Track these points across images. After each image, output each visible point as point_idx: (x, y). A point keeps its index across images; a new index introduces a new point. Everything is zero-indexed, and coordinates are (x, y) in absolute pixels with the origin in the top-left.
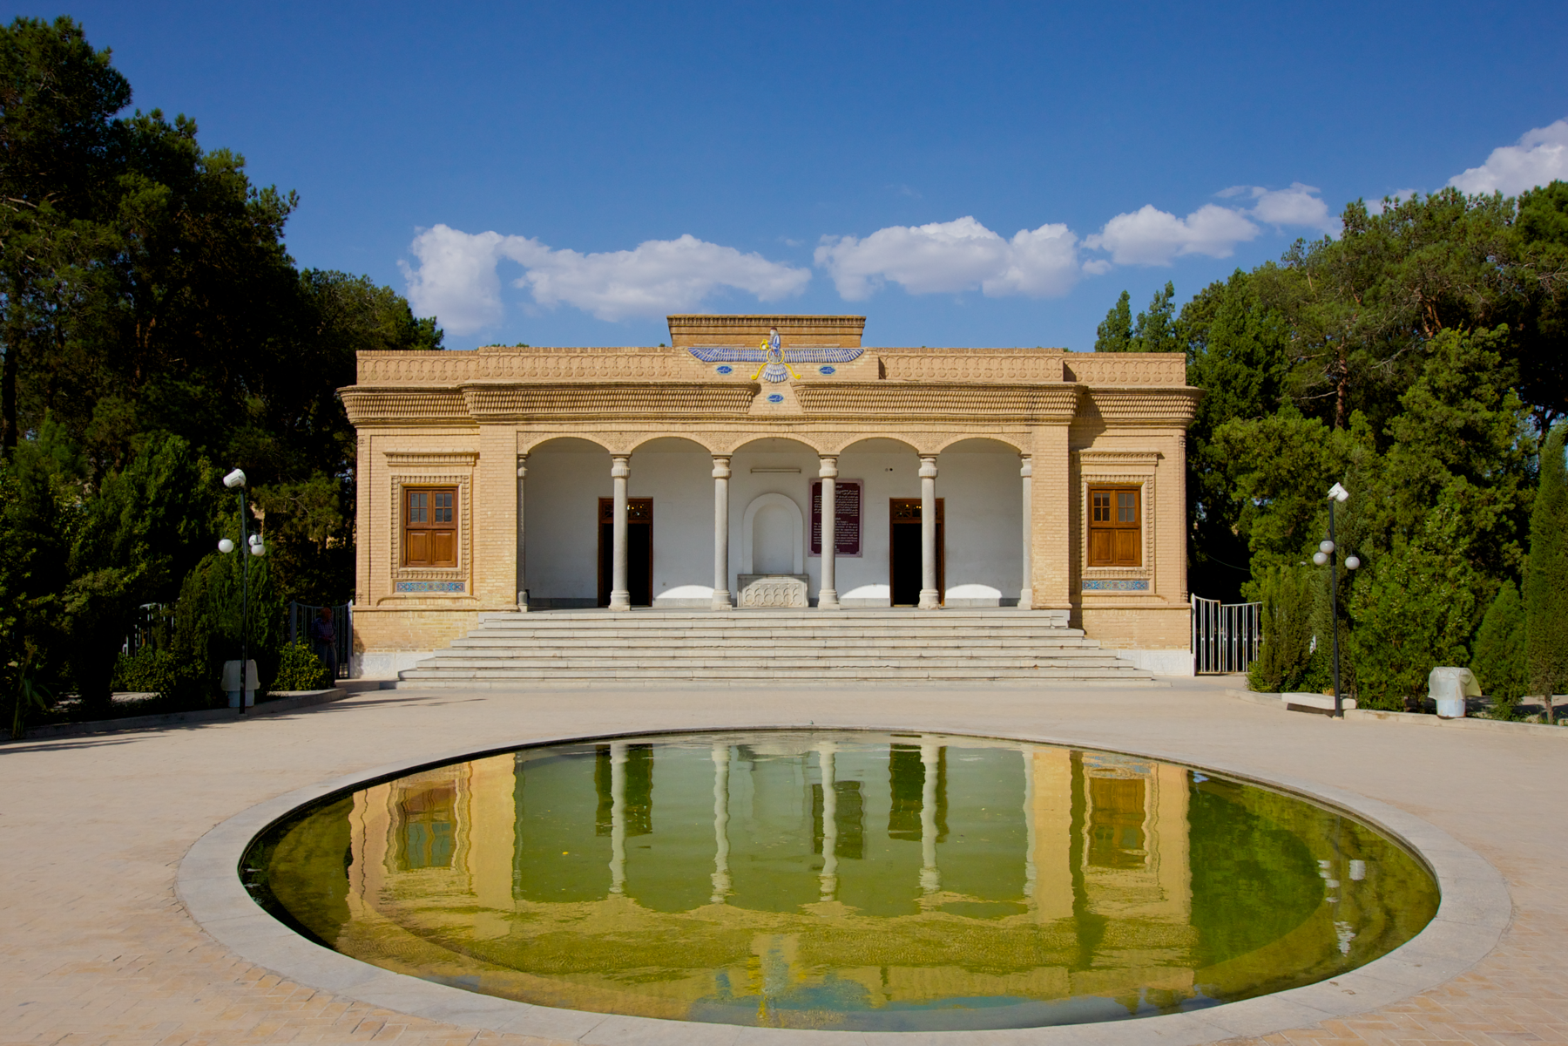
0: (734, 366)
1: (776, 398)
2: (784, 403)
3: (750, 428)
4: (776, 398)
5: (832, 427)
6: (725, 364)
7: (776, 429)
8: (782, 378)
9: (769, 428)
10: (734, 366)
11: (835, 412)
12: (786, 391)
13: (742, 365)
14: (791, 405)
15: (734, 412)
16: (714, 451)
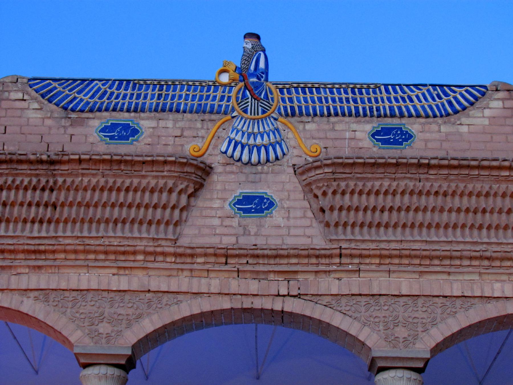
0: (146, 123)
1: (255, 205)
2: (277, 217)
3: (182, 282)
4: (255, 205)
5: (405, 283)
6: (123, 117)
7: (254, 286)
8: (272, 155)
9: (235, 285)
10: (146, 123)
11: (416, 240)
12: (280, 185)
13: (170, 123)
14: (293, 222)
15: (141, 238)
16: (79, 339)
